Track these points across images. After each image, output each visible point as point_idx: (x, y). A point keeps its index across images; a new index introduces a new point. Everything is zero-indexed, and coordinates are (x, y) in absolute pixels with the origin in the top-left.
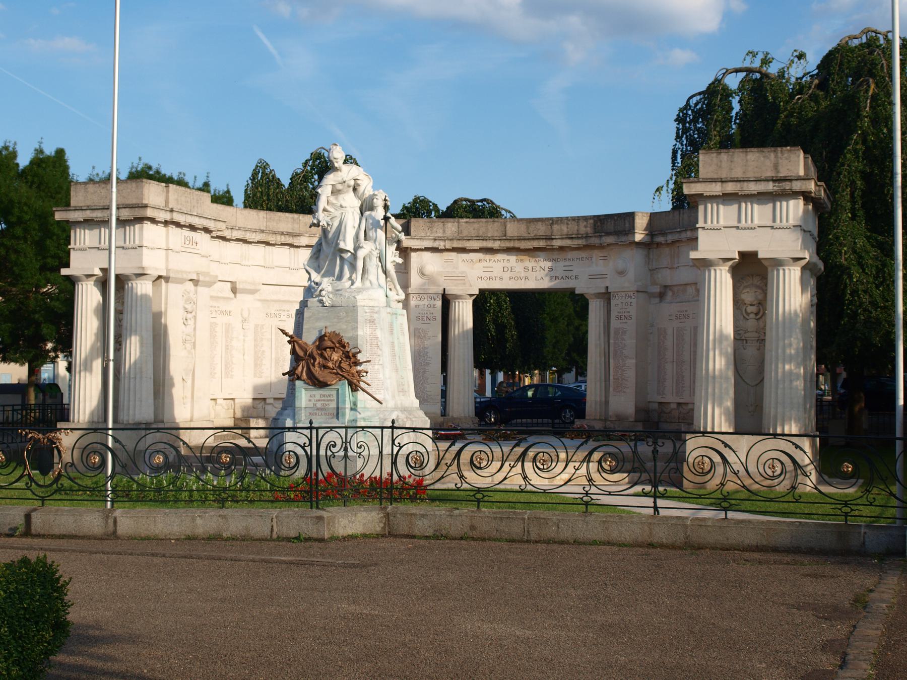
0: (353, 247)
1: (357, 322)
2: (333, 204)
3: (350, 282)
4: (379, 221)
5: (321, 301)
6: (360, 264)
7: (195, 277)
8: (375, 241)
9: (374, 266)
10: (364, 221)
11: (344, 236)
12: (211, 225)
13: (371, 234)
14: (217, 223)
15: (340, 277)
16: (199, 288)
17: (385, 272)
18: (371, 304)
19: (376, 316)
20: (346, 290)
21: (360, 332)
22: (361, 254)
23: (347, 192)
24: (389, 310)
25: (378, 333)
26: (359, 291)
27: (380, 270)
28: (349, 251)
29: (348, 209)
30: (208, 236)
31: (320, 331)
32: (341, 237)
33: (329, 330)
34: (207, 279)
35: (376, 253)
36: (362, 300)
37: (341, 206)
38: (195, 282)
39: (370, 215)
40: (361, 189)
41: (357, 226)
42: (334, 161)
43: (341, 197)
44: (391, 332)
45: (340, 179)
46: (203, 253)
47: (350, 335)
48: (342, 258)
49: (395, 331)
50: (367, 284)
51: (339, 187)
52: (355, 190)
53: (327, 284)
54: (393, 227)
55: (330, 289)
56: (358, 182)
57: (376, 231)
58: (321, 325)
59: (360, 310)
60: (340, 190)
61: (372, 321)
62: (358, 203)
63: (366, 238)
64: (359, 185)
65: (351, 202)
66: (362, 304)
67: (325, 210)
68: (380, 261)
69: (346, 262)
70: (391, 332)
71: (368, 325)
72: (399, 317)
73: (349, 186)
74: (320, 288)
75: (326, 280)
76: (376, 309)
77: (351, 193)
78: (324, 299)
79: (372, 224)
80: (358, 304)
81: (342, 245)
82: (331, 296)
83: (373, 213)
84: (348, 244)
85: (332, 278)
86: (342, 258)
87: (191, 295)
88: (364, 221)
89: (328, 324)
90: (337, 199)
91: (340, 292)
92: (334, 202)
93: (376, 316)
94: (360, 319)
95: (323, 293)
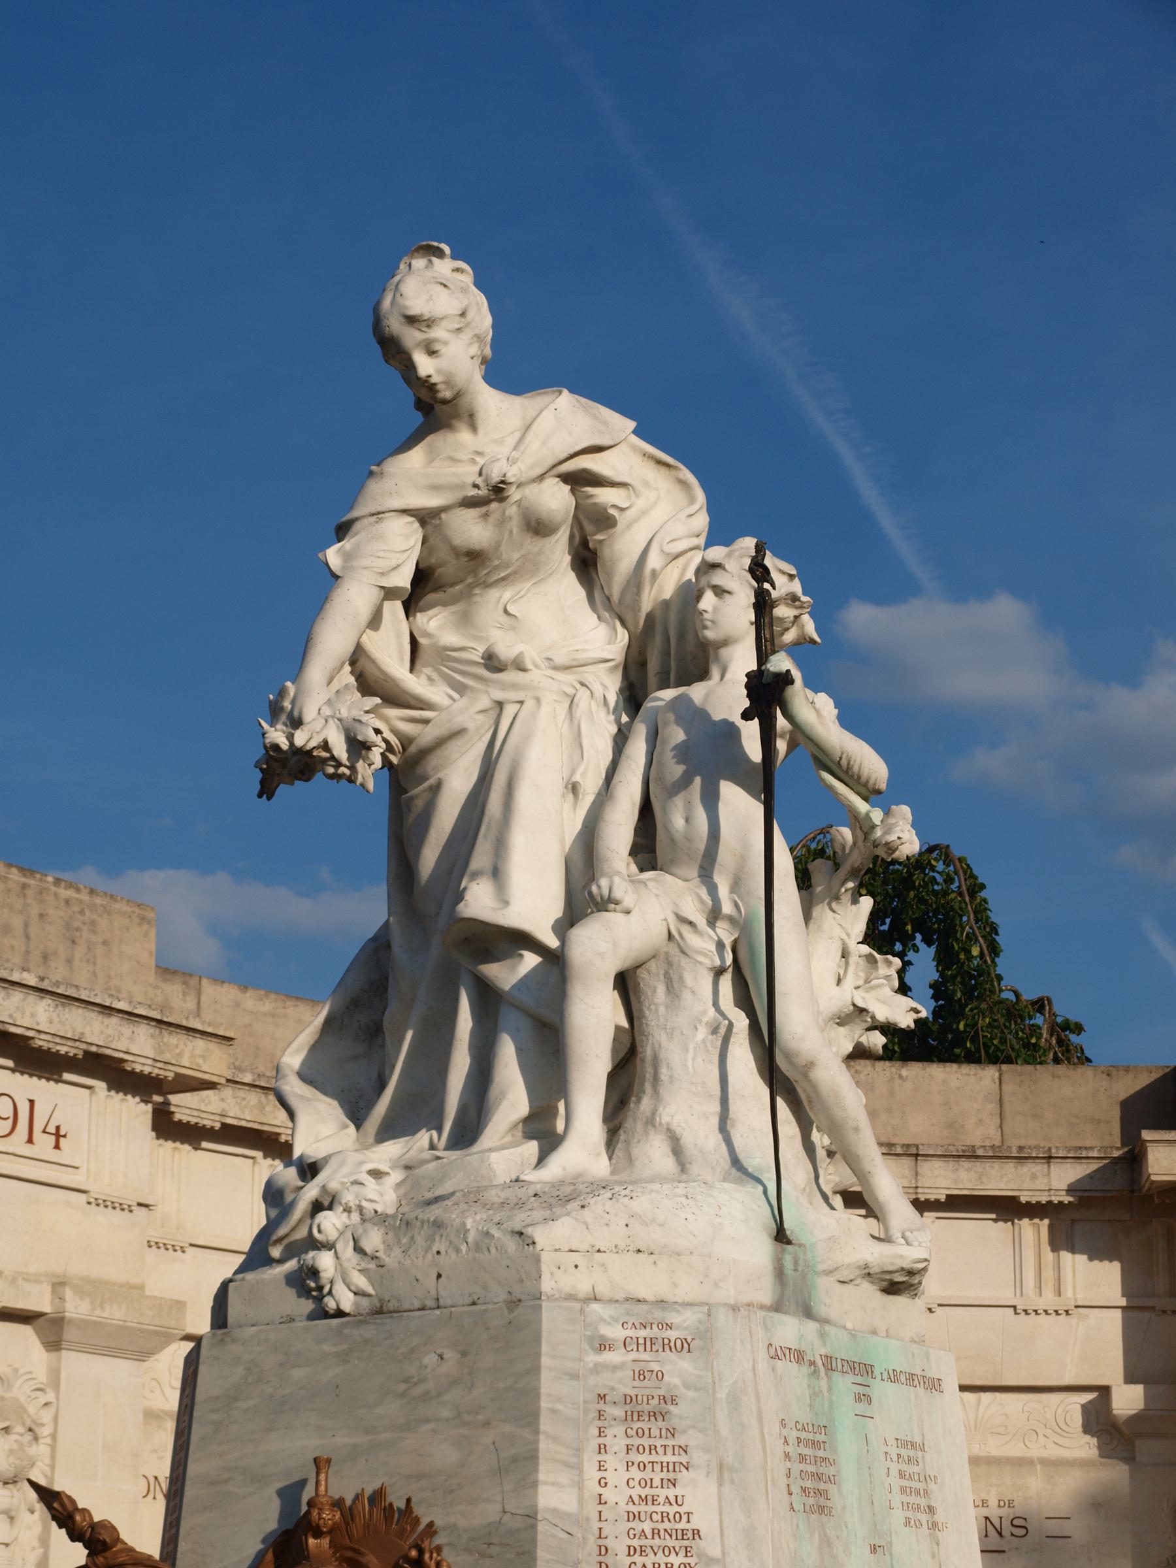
0: (556, 909)
1: (530, 1418)
2: (444, 655)
3: (533, 1147)
4: (730, 733)
5: (306, 1282)
6: (594, 1018)
7: (39, 1301)
8: (706, 874)
9: (694, 1027)
10: (638, 748)
11: (500, 846)
12: (140, 1048)
13: (682, 818)
14: (175, 1040)
15: (467, 1133)
16: (73, 1363)
17: (780, 1078)
18: (648, 1281)
19: (677, 1370)
20: (475, 1197)
21: (554, 1495)
22: (599, 948)
23: (530, 569)
24: (790, 1330)
25: (699, 1497)
26: (567, 1196)
27: (743, 1058)
28: (522, 940)
29: (535, 676)
30: (135, 1113)
31: (290, 1494)
32: (481, 858)
33: (345, 1485)
34: (114, 1313)
35: (705, 945)
36: (577, 1259)
37: (493, 663)
38: (51, 1329)
39: (684, 700)
40: (623, 549)
41: (591, 785)
42: (411, 337)
43: (491, 603)
44: (815, 1490)
45: (468, 473)
46: (97, 1189)
47: (486, 1512)
48: (488, 1000)
49: (848, 1494)
50: (654, 1153)
51: (471, 529)
52: (586, 562)
53: (362, 1168)
54: (824, 760)
55: (384, 1196)
56: (604, 496)
57: (711, 799)
58: (290, 1448)
59: (551, 1319)
60: (475, 557)
61: (649, 1412)
62: (604, 642)
63: (648, 848)
64: (605, 520)
65: (557, 630)
66: (583, 1285)
67: (369, 681)
68: (744, 1000)
69: (508, 1016)
70: (815, 1490)
71: (616, 1439)
72: (882, 1390)
73: (538, 527)
74: (311, 1191)
75: (393, 1149)
76: (684, 1321)
77: (569, 586)
78: (325, 1262)
79: (683, 753)
80: (547, 1285)
81: (478, 902)
82: (373, 1240)
83: (697, 692)
84: (524, 892)
85: (423, 1138)
86: (488, 1000)
87: (20, 1391)
88: (638, 748)
89: (340, 1440)
90: (465, 621)
91: (435, 1212)
92: (451, 638)
93: (677, 1370)
94: (554, 1388)
95: (330, 1223)
